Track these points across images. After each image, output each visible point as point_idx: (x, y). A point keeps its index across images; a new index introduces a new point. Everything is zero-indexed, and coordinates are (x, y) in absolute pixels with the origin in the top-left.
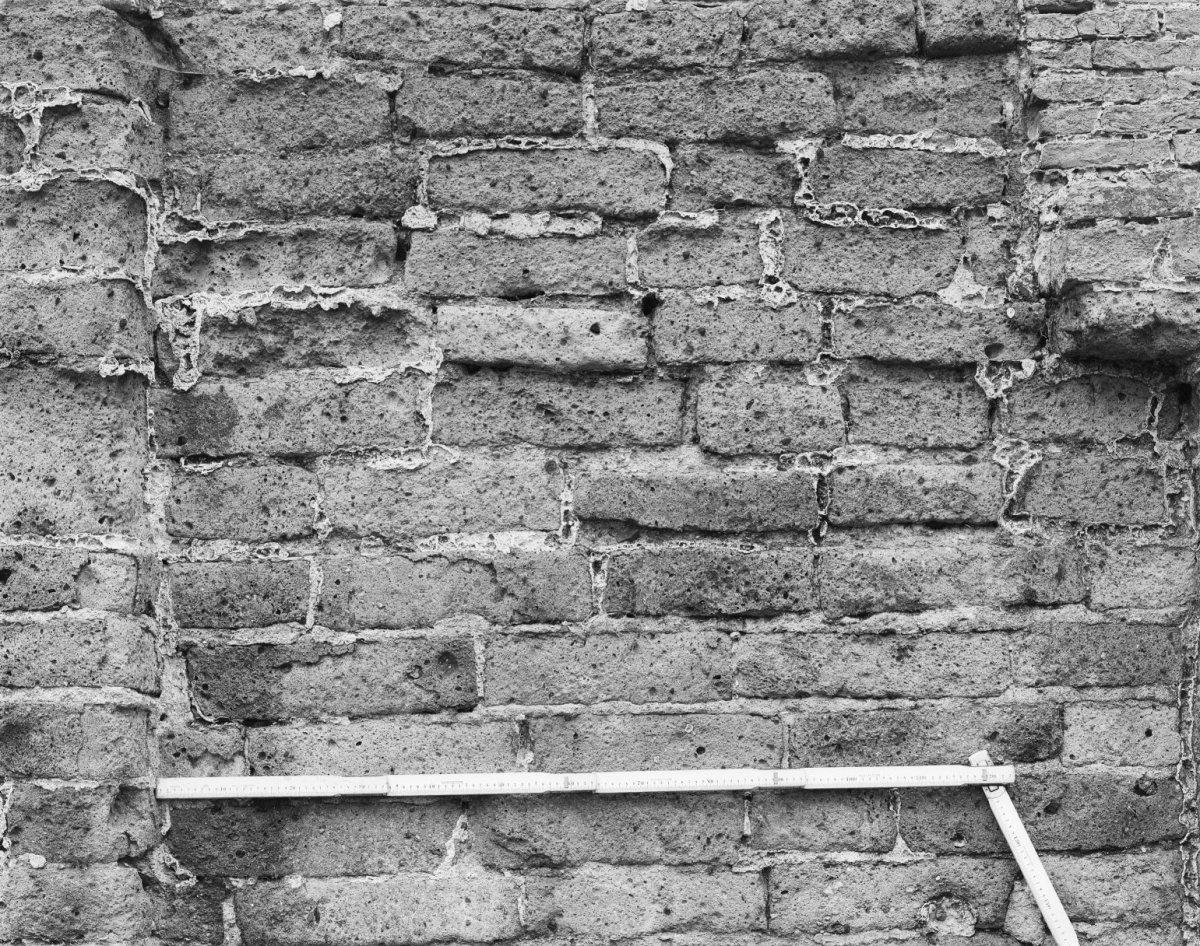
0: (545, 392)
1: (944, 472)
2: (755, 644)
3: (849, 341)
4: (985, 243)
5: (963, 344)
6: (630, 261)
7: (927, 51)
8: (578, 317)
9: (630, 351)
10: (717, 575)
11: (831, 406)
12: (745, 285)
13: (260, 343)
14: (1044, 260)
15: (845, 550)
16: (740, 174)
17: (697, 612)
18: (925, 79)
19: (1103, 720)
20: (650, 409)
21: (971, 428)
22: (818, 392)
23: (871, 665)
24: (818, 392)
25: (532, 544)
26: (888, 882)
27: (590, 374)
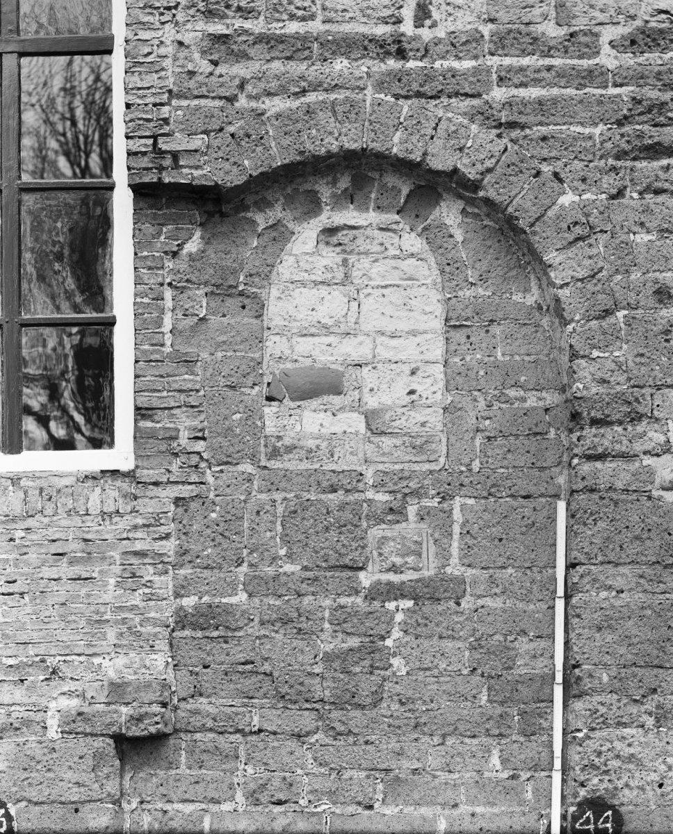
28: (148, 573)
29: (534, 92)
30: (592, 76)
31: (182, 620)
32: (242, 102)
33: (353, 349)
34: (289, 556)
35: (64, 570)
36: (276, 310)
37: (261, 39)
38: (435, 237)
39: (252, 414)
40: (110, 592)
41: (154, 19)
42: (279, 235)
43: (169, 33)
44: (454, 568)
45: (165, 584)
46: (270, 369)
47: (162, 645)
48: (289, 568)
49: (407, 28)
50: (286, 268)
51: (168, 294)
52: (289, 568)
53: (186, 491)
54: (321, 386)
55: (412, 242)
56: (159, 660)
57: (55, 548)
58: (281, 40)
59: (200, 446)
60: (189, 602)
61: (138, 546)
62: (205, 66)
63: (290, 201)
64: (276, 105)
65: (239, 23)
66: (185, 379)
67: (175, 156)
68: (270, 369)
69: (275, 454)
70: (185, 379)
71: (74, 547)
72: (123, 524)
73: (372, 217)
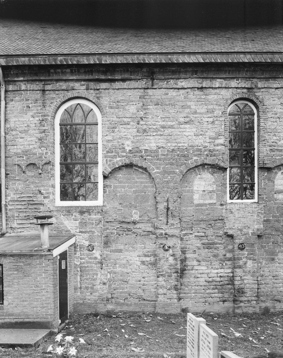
0: (199, 237)
1: (220, 241)
2: (210, 250)
3: (215, 235)
4: (222, 230)
5: (221, 235)
6: (204, 230)
7: (219, 220)
8: (201, 233)
9: (204, 235)
10: (209, 247)
11: (214, 238)
12: (210, 232)
13: (185, 235)
14: (225, 231)
15: (215, 245)
16: (210, 226)
17: (207, 248)
18: (219, 221)
19: (228, 254)
20: (205, 238)
21: (222, 239)
22: (214, 237)
23: (216, 251)
24: (214, 237)
25: (199, 245)
26: (217, 262)
27: (202, 236)
28: (260, 215)
31: (264, 221)
32: (274, 157)
34: (278, 213)
35: (250, 214)
36: (276, 182)
37: (276, 149)
39: (273, 195)
40: (255, 217)
41: (263, 147)
42: (276, 173)
43: (265, 149)
45: (262, 216)
47: (262, 224)
48: (277, 214)
50: (277, 177)
51: (263, 180)
52: (277, 214)
53: (265, 205)
56: (262, 226)
57: (249, 212)
58: (279, 150)
59: (267, 199)
60: (265, 219)
61: (259, 212)
62: (269, 153)
63: (277, 169)
64: (278, 158)
65: (273, 147)
66: (265, 191)
67: (266, 164)
68: (275, 190)
69: (276, 200)
70: (265, 191)
71: (251, 212)
72: (257, 209)
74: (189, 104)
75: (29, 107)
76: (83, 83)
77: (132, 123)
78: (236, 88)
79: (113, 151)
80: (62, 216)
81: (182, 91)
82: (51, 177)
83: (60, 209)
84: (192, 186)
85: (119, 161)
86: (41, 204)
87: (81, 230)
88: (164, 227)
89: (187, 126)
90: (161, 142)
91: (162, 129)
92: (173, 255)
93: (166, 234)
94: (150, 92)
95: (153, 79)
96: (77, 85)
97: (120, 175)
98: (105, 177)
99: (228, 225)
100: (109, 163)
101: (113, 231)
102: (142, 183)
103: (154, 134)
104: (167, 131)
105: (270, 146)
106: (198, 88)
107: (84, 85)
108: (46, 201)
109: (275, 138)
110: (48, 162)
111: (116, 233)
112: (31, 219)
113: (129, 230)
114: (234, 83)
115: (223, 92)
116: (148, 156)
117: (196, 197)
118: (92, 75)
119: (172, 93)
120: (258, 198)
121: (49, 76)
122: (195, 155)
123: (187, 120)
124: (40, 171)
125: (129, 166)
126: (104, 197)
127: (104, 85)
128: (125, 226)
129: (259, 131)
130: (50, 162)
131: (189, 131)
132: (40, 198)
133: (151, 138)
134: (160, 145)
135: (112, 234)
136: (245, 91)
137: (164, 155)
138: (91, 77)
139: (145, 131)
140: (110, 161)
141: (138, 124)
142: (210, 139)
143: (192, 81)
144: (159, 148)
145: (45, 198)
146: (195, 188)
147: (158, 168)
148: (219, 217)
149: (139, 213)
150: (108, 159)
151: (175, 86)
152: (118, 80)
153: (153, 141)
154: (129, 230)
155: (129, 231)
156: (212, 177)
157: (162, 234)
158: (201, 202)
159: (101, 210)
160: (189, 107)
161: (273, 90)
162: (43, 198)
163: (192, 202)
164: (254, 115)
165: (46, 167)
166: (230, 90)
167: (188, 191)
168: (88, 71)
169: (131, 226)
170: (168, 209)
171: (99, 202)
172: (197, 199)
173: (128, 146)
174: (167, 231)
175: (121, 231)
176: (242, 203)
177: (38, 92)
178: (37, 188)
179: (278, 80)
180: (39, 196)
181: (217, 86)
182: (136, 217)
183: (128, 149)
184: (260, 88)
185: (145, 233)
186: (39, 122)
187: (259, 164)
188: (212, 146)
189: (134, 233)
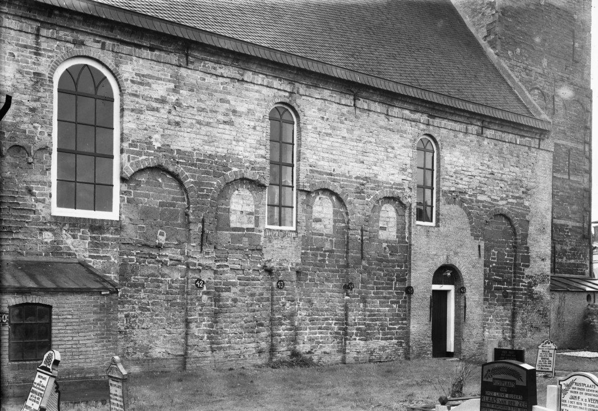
8: (237, 266)
13: (219, 266)
21: (258, 274)
24: (251, 271)
29: (345, 183)
30: (352, 182)
33: (323, 215)
36: (314, 208)
38: (332, 200)
39: (311, 224)
42: (315, 197)
44: (334, 249)
46: (313, 217)
49: (332, 172)
54: (318, 220)
55: (330, 201)
64: (317, 181)
73: (325, 197)
74: (229, 97)
75: (14, 56)
76: (97, 39)
77: (162, 111)
78: (279, 90)
79: (137, 145)
80: (64, 232)
81: (221, 80)
82: (47, 170)
83: (60, 221)
84: (228, 204)
85: (145, 160)
86: (30, 210)
87: (92, 254)
88: (198, 256)
89: (227, 127)
90: (198, 143)
91: (198, 126)
92: (207, 293)
93: (200, 265)
94: (183, 71)
95: (187, 56)
96: (89, 41)
97: (143, 178)
98: (123, 180)
99: (267, 257)
100: (131, 161)
101: (132, 257)
102: (170, 193)
103: (189, 130)
104: (205, 129)
105: (310, 166)
106: (238, 80)
107: (98, 42)
108: (39, 206)
109: (315, 157)
110: (44, 147)
111: (135, 261)
112: (14, 232)
113: (151, 256)
114: (276, 83)
115: (265, 91)
116: (181, 158)
117: (233, 218)
118: (112, 32)
119: (210, 80)
120: (297, 225)
121: (49, 16)
122: (235, 166)
123: (226, 119)
124: (31, 160)
125: (158, 169)
126: (120, 208)
127: (126, 49)
128: (146, 250)
129: (299, 145)
130: (47, 147)
131: (227, 133)
132: (30, 200)
133: (186, 135)
134: (196, 147)
135: (130, 261)
136: (287, 94)
137: (200, 161)
138: (111, 35)
139: (177, 124)
140: (134, 158)
141: (169, 113)
142: (251, 147)
143: (231, 69)
144: (195, 150)
145: (37, 201)
146: (233, 207)
147: (193, 177)
148: (257, 246)
149: (165, 234)
150: (131, 155)
151: (213, 71)
152: (145, 47)
153: (187, 139)
154: (151, 256)
155: (152, 258)
156: (251, 195)
157: (195, 265)
158: (239, 225)
159: (118, 226)
160: (228, 102)
161: (314, 100)
162: (33, 200)
163: (229, 225)
164: (293, 123)
165: (39, 155)
166: (274, 90)
167: (225, 209)
168: (108, 27)
169: (154, 252)
170: (203, 231)
171: (113, 215)
172: (235, 221)
173: (156, 141)
174: (201, 262)
175: (142, 257)
176: (281, 231)
177: (30, 36)
178: (25, 185)
179: (318, 89)
180: (28, 197)
181: (259, 83)
182: (162, 240)
183: (157, 145)
184: (301, 95)
185: (172, 262)
186: (32, 83)
187: (298, 185)
188: (253, 156)
189: (159, 261)
